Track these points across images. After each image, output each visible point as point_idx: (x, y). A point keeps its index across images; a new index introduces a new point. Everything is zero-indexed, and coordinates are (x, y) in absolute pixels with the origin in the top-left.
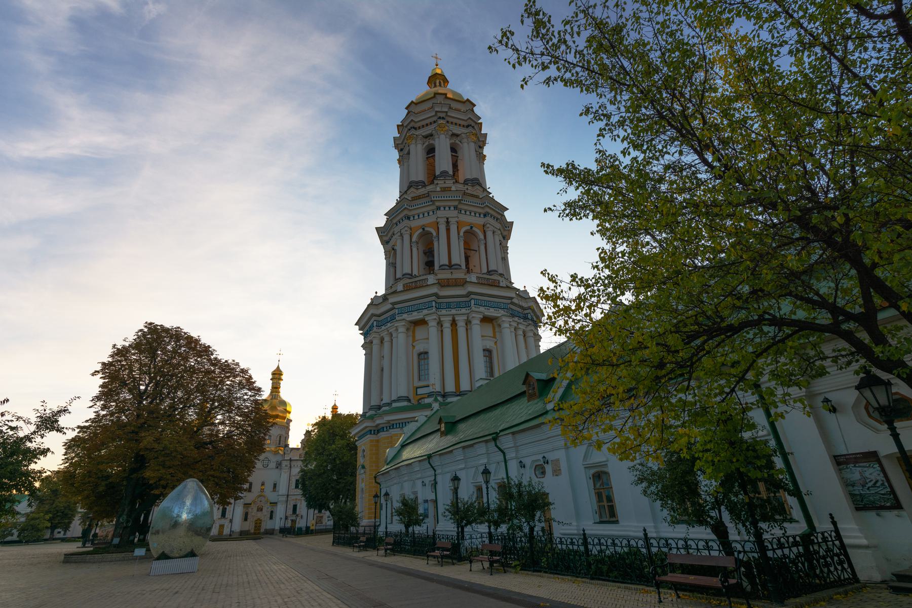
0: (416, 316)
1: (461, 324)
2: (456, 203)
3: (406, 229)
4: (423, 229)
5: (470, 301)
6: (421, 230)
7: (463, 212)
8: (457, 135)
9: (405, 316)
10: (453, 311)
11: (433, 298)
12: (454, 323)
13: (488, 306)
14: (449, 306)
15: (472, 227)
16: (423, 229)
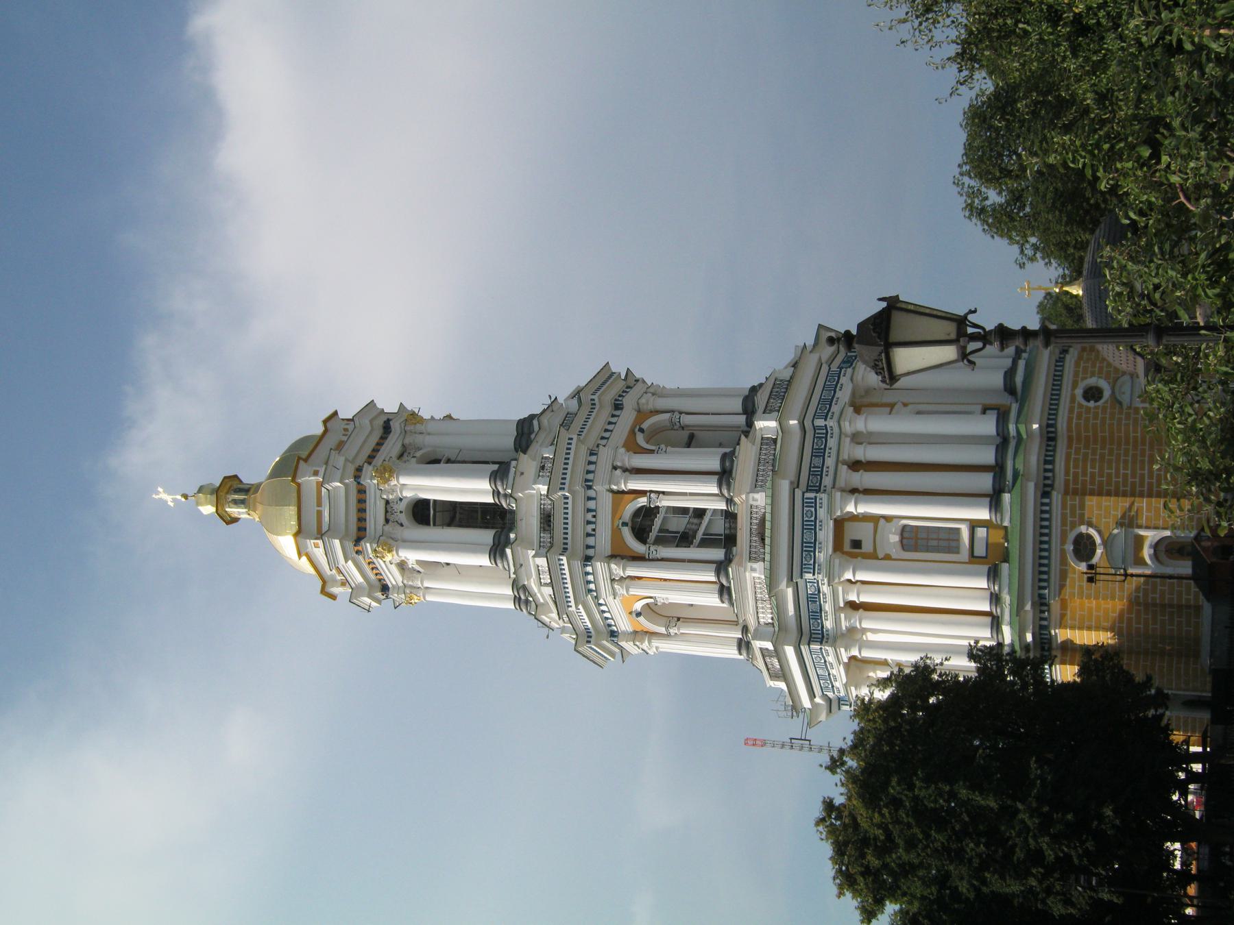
0: (839, 673)
1: (852, 597)
2: (577, 564)
3: (637, 643)
4: (638, 614)
5: (806, 579)
6: (641, 619)
7: (591, 541)
8: (387, 502)
9: (837, 684)
10: (828, 607)
11: (804, 649)
12: (853, 606)
13: (810, 547)
14: (817, 614)
15: (625, 524)
16: (638, 614)
